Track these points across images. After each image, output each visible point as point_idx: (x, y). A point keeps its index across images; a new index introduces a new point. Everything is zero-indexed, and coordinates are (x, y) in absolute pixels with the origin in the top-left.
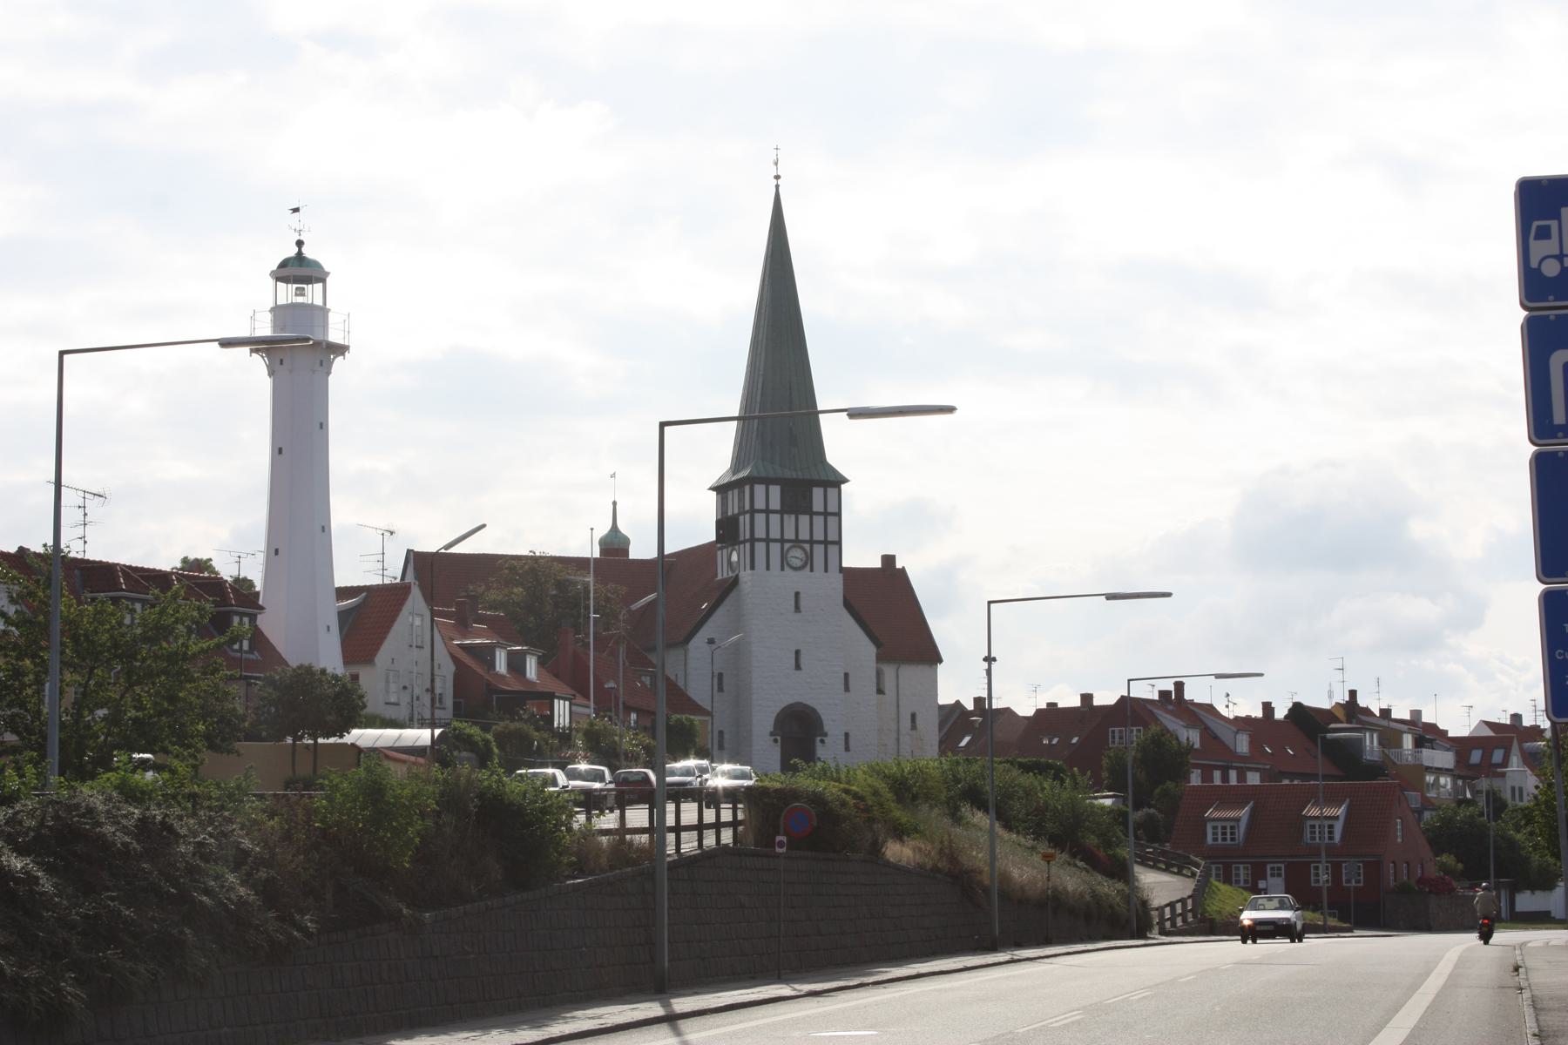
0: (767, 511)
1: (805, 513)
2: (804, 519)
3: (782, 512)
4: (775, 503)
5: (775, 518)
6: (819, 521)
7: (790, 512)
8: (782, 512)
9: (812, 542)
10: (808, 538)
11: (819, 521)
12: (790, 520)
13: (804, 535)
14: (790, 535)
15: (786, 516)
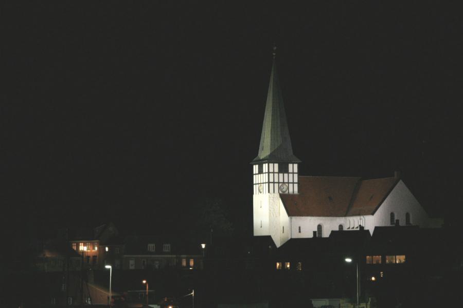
0: (274, 173)
1: (286, 173)
2: (286, 175)
3: (279, 173)
4: (276, 170)
5: (276, 175)
6: (291, 175)
7: (281, 173)
8: (279, 173)
9: (288, 183)
10: (287, 181)
11: (291, 175)
12: (281, 175)
13: (286, 181)
14: (281, 180)
15: (280, 174)
